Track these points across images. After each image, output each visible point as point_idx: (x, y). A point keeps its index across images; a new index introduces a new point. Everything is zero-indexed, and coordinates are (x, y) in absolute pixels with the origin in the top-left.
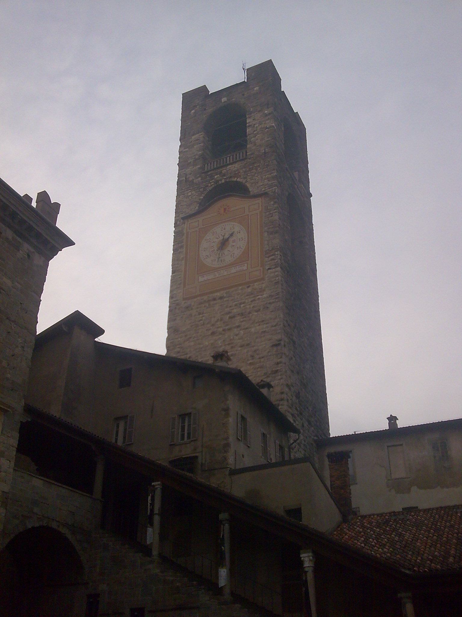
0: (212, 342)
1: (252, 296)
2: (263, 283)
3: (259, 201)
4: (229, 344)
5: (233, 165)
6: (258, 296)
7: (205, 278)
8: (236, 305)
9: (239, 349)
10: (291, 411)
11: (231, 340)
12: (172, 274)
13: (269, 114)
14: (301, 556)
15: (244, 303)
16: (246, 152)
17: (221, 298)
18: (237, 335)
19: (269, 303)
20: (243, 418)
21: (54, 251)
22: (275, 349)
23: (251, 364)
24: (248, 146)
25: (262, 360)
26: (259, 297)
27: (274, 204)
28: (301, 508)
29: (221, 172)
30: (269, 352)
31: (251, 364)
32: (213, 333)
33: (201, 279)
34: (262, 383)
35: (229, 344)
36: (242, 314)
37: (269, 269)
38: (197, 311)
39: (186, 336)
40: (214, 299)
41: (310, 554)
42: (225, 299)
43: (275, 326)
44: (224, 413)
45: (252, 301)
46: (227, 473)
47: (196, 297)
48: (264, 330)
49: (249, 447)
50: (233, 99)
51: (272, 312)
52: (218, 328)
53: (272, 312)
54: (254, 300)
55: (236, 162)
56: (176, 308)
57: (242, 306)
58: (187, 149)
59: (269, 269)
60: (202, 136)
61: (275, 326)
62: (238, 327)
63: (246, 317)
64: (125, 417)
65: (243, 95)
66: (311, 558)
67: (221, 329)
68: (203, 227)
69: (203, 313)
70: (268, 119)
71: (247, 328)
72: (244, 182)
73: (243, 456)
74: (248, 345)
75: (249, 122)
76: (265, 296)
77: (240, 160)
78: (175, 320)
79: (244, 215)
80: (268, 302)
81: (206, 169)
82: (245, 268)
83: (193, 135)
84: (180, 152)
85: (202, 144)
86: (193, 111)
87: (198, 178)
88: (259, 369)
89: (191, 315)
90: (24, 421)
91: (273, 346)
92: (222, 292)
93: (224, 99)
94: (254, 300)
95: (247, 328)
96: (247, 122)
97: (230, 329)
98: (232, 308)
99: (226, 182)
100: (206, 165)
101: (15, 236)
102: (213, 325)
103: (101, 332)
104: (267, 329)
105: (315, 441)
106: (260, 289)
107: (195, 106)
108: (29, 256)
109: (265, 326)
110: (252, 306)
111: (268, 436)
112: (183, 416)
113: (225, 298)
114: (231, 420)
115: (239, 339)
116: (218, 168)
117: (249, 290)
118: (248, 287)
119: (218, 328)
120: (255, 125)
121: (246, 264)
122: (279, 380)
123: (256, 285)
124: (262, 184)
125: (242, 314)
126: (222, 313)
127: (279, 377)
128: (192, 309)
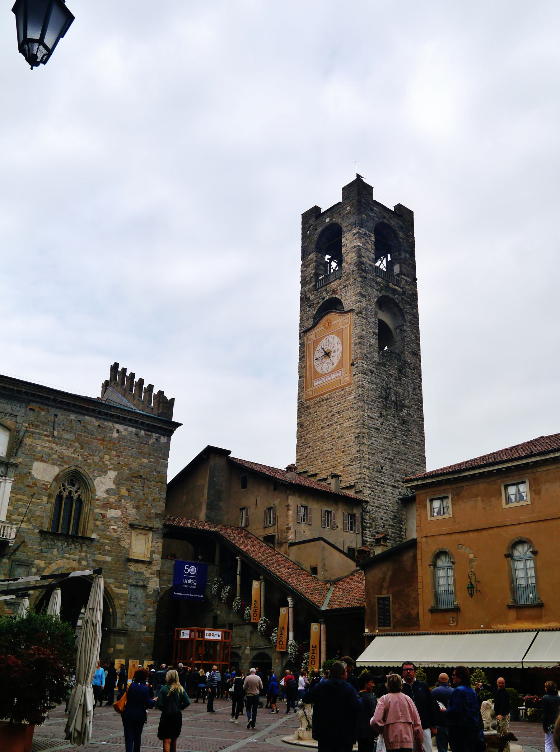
0: (322, 434)
1: (345, 397)
2: (351, 387)
3: (349, 315)
4: (331, 436)
5: (334, 283)
6: (348, 397)
7: (317, 383)
8: (335, 405)
9: (337, 440)
10: (368, 485)
11: (332, 433)
12: (299, 379)
13: (356, 233)
14: (288, 599)
15: (339, 404)
16: (342, 269)
17: (327, 399)
18: (336, 429)
19: (354, 403)
20: (306, 508)
21: (172, 432)
22: (357, 439)
23: (343, 452)
24: (343, 265)
25: (349, 448)
26: (349, 398)
27: (358, 319)
28: (317, 567)
29: (326, 290)
30: (353, 442)
31: (343, 452)
32: (322, 428)
33: (315, 384)
34: (332, 475)
35: (331, 436)
36: (338, 413)
37: (354, 375)
38: (313, 410)
39: (307, 430)
40: (323, 401)
41: (291, 599)
42: (329, 400)
43: (357, 422)
44: (286, 508)
45: (344, 402)
46: (287, 544)
47: (312, 398)
48: (350, 425)
49: (310, 525)
50: (334, 219)
51: (356, 410)
52: (325, 423)
53: (356, 410)
54: (345, 401)
55: (335, 280)
56: (301, 408)
57: (339, 405)
58: (305, 269)
59: (354, 375)
60: (315, 255)
61: (357, 422)
62: (336, 422)
63: (340, 415)
64: (244, 509)
65: (340, 214)
66: (291, 600)
67: (326, 425)
68: (317, 338)
69: (317, 412)
70: (355, 239)
71: (341, 424)
72: (340, 299)
73: (304, 532)
74: (342, 437)
75: (344, 242)
76: (352, 397)
77: (338, 279)
78: (301, 417)
79: (339, 328)
80: (354, 402)
81: (318, 287)
82: (340, 374)
83: (309, 255)
84: (302, 271)
85: (314, 264)
86: (308, 232)
87: (312, 295)
88: (348, 456)
89: (310, 413)
90: (166, 532)
91: (356, 438)
92: (327, 394)
93: (328, 220)
94: (345, 401)
95: (341, 424)
96: (343, 241)
97: (331, 425)
98: (333, 407)
99: (329, 299)
100: (318, 283)
101: (147, 432)
102: (322, 421)
103: (230, 452)
104: (352, 425)
105: (401, 499)
106: (349, 392)
107: (310, 227)
108: (157, 440)
109: (352, 421)
110: (344, 406)
111: (333, 512)
112: (270, 509)
113: (329, 399)
114: (290, 512)
115: (337, 432)
116: (324, 286)
117: (343, 392)
118: (342, 390)
119: (325, 423)
120: (347, 244)
121: (341, 371)
122: (359, 463)
123: (347, 389)
124: (351, 300)
125: (338, 413)
126: (328, 412)
127: (359, 461)
128: (310, 409)
